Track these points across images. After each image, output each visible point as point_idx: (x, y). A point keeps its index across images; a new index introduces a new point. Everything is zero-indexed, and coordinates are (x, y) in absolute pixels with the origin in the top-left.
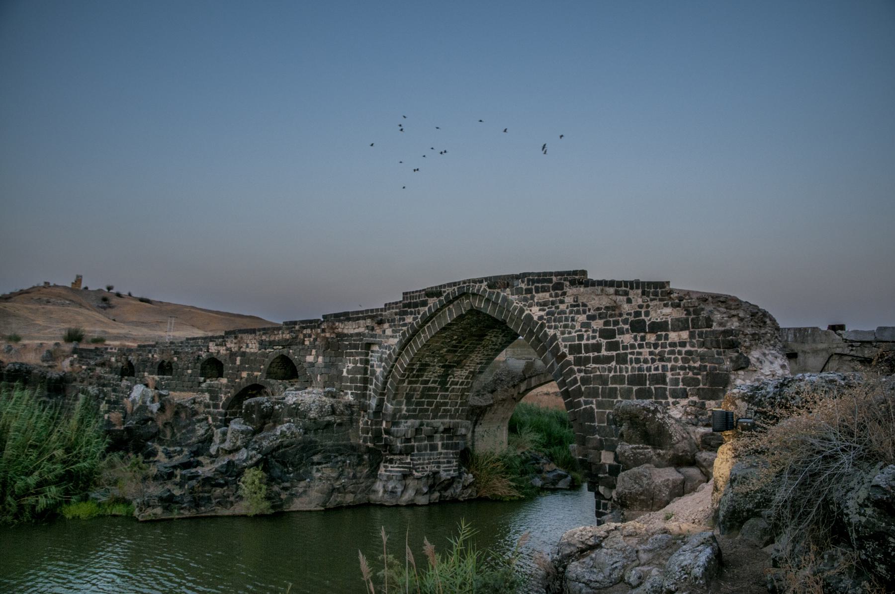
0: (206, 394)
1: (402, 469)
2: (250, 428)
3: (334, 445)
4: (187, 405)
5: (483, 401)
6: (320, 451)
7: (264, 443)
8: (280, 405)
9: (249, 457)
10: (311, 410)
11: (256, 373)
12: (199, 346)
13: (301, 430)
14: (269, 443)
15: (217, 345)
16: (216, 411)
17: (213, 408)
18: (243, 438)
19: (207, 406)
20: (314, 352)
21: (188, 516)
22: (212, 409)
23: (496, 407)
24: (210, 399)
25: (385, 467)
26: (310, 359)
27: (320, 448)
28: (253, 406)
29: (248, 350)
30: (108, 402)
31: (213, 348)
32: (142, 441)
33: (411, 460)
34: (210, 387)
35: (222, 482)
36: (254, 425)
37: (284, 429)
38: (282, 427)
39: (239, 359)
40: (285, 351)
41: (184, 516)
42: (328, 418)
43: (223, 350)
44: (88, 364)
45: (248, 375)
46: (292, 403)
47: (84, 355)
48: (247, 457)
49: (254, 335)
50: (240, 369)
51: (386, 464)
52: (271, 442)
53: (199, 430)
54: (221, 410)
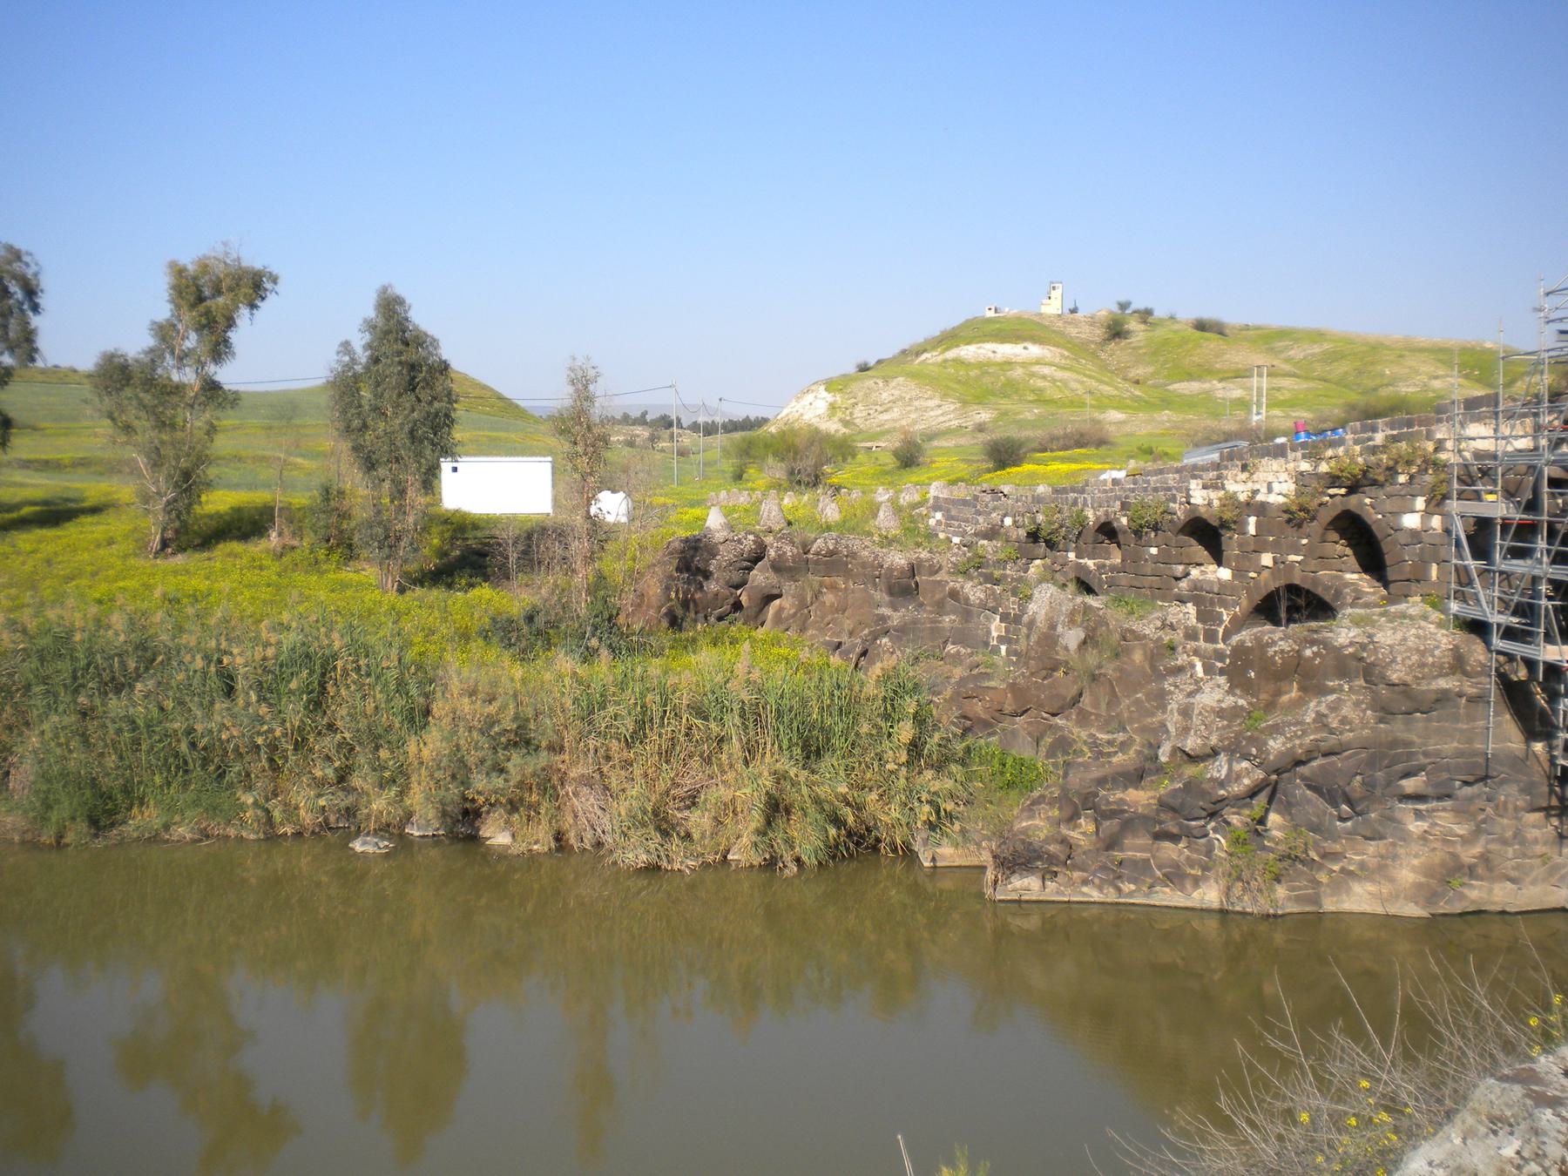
0: (1190, 605)
2: (1241, 702)
3: (1459, 754)
6: (1422, 768)
7: (1271, 743)
8: (1315, 649)
9: (1234, 776)
10: (1393, 661)
12: (1169, 489)
13: (1369, 712)
14: (1284, 744)
15: (1205, 487)
16: (1210, 646)
17: (1205, 641)
18: (1224, 728)
19: (1191, 635)
20: (1420, 503)
21: (1097, 899)
22: (1202, 644)
27: (1423, 760)
31: (1199, 496)
32: (1045, 715)
34: (1196, 588)
35: (1175, 830)
36: (1253, 696)
37: (1323, 709)
39: (1252, 520)
40: (1353, 502)
41: (1092, 900)
42: (1443, 683)
43: (1215, 496)
44: (963, 534)
45: (1275, 561)
48: (1228, 775)
49: (1282, 460)
52: (1290, 739)
53: (1171, 693)
54: (1221, 646)
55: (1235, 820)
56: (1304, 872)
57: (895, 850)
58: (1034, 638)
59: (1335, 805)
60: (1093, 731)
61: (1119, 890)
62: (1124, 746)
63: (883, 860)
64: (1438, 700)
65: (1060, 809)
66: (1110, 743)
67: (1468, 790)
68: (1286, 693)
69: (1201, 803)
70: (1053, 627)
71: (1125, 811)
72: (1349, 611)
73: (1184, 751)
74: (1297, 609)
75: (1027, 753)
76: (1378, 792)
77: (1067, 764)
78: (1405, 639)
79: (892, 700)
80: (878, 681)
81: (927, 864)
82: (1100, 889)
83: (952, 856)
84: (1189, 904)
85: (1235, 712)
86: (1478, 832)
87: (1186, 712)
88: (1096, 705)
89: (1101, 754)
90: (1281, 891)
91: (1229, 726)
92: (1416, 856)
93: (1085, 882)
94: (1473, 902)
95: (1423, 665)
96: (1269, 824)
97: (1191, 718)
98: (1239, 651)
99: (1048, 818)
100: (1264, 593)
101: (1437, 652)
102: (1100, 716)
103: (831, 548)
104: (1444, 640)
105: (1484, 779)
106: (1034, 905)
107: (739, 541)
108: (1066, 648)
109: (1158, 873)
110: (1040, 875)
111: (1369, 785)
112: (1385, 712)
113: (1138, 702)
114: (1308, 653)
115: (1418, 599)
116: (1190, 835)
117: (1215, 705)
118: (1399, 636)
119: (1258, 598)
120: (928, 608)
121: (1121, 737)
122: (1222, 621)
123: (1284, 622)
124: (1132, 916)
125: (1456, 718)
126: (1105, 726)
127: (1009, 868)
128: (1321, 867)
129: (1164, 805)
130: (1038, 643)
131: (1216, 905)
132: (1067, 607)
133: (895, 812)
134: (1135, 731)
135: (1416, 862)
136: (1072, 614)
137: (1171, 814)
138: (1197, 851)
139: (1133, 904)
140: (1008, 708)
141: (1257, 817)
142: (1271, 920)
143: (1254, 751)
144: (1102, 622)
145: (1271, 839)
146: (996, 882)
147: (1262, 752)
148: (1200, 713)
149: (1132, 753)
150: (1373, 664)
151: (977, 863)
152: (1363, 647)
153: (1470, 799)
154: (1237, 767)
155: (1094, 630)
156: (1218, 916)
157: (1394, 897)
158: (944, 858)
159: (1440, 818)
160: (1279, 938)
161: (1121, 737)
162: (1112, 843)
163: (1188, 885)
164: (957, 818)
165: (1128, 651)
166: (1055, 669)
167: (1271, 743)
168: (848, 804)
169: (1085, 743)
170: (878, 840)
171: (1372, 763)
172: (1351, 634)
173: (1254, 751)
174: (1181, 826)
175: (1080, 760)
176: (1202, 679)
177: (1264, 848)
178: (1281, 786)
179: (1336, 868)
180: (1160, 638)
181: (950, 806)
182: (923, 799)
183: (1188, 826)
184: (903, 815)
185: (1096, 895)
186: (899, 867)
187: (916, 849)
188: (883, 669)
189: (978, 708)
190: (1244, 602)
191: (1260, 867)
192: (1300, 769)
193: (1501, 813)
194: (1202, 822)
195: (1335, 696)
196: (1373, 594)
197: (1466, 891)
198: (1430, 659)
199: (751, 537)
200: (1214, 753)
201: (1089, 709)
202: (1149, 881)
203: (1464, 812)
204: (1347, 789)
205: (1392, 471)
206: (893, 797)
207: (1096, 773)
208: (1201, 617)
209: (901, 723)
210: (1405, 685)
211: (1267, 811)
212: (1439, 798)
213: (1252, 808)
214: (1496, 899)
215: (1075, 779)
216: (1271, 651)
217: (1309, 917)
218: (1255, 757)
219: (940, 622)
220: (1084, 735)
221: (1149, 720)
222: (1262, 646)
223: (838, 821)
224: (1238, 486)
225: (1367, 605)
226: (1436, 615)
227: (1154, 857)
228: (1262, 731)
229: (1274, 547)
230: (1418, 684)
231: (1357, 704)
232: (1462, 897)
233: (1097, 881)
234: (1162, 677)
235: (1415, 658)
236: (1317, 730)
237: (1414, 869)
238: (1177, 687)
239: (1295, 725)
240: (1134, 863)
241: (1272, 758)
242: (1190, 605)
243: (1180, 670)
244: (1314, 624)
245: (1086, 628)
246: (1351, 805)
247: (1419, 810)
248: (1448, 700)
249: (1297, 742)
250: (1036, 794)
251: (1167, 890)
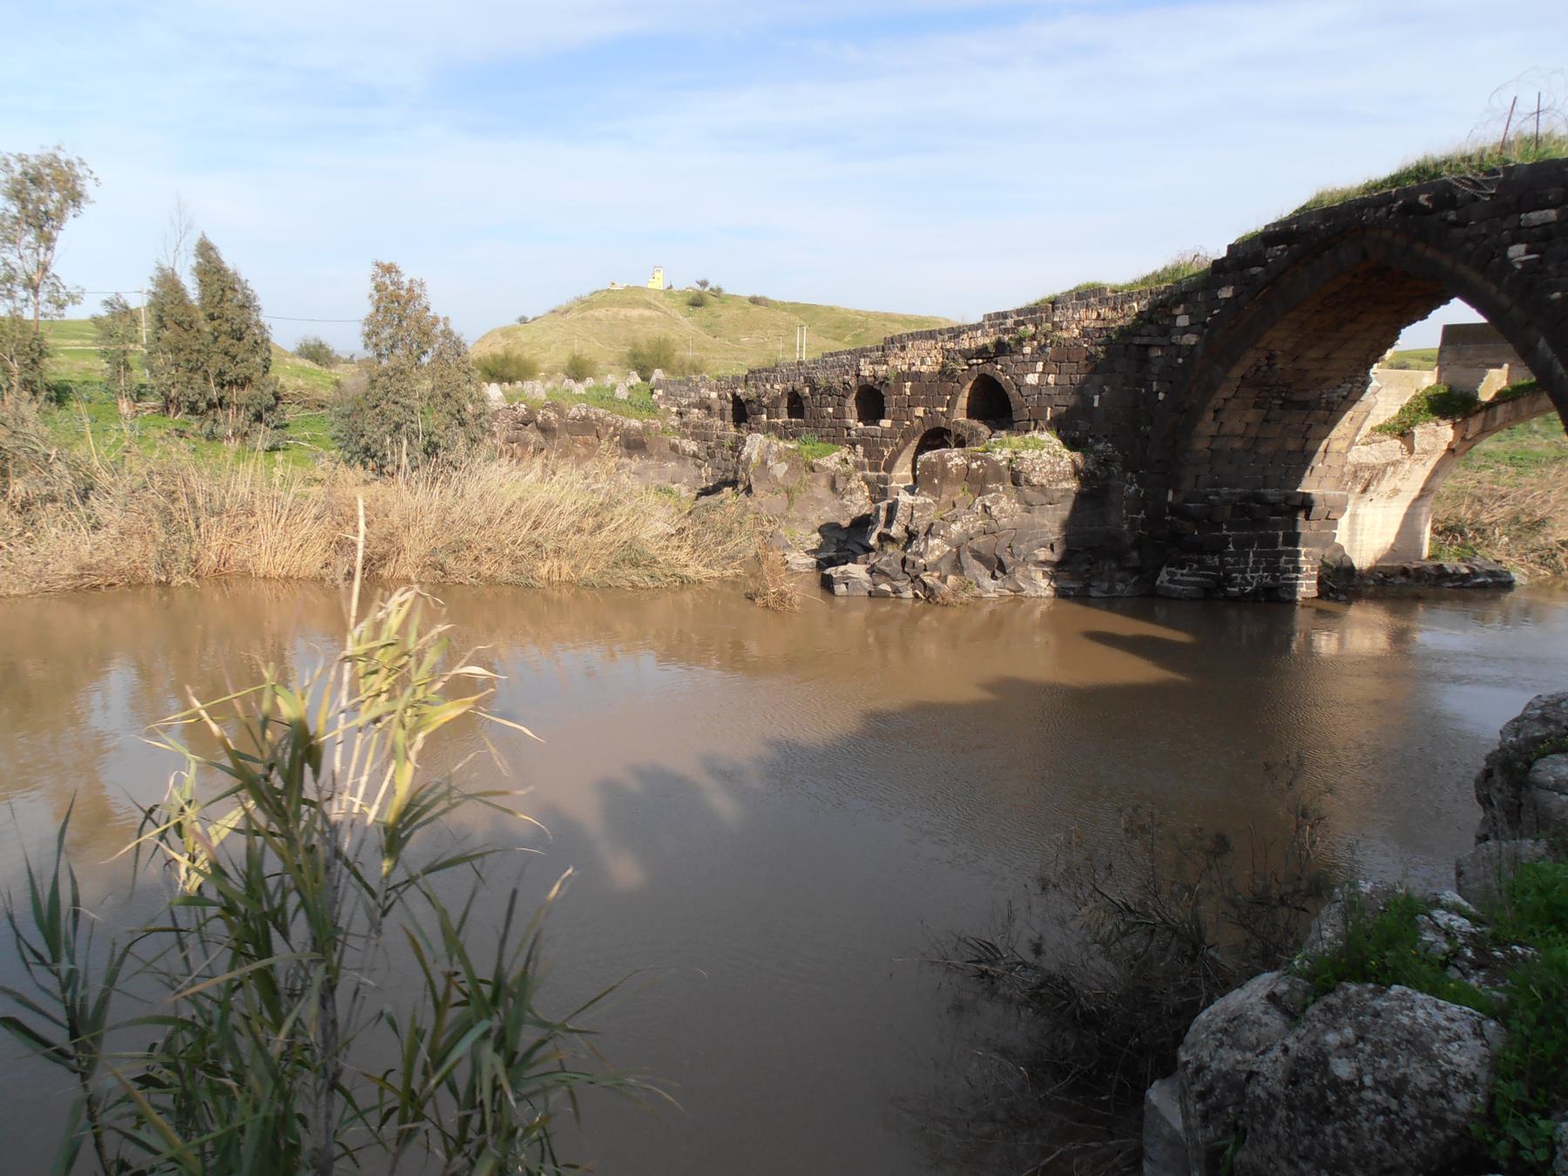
1: (1198, 579)
2: (928, 500)
5: (1377, 454)
8: (979, 463)
10: (1034, 469)
15: (871, 363)
20: (1040, 366)
23: (1407, 467)
25: (1168, 573)
26: (1032, 379)
29: (924, 369)
31: (866, 371)
33: (1221, 562)
47: (671, 389)
50: (912, 404)
51: (1169, 569)
70: (764, 463)
95: (1054, 472)
107: (514, 409)
114: (974, 465)
122: (884, 456)
195: (993, 495)
199: (523, 406)
205: (1020, 341)
208: (867, 454)
210: (1042, 485)
216: (949, 465)
229: (925, 403)
235: (1048, 467)
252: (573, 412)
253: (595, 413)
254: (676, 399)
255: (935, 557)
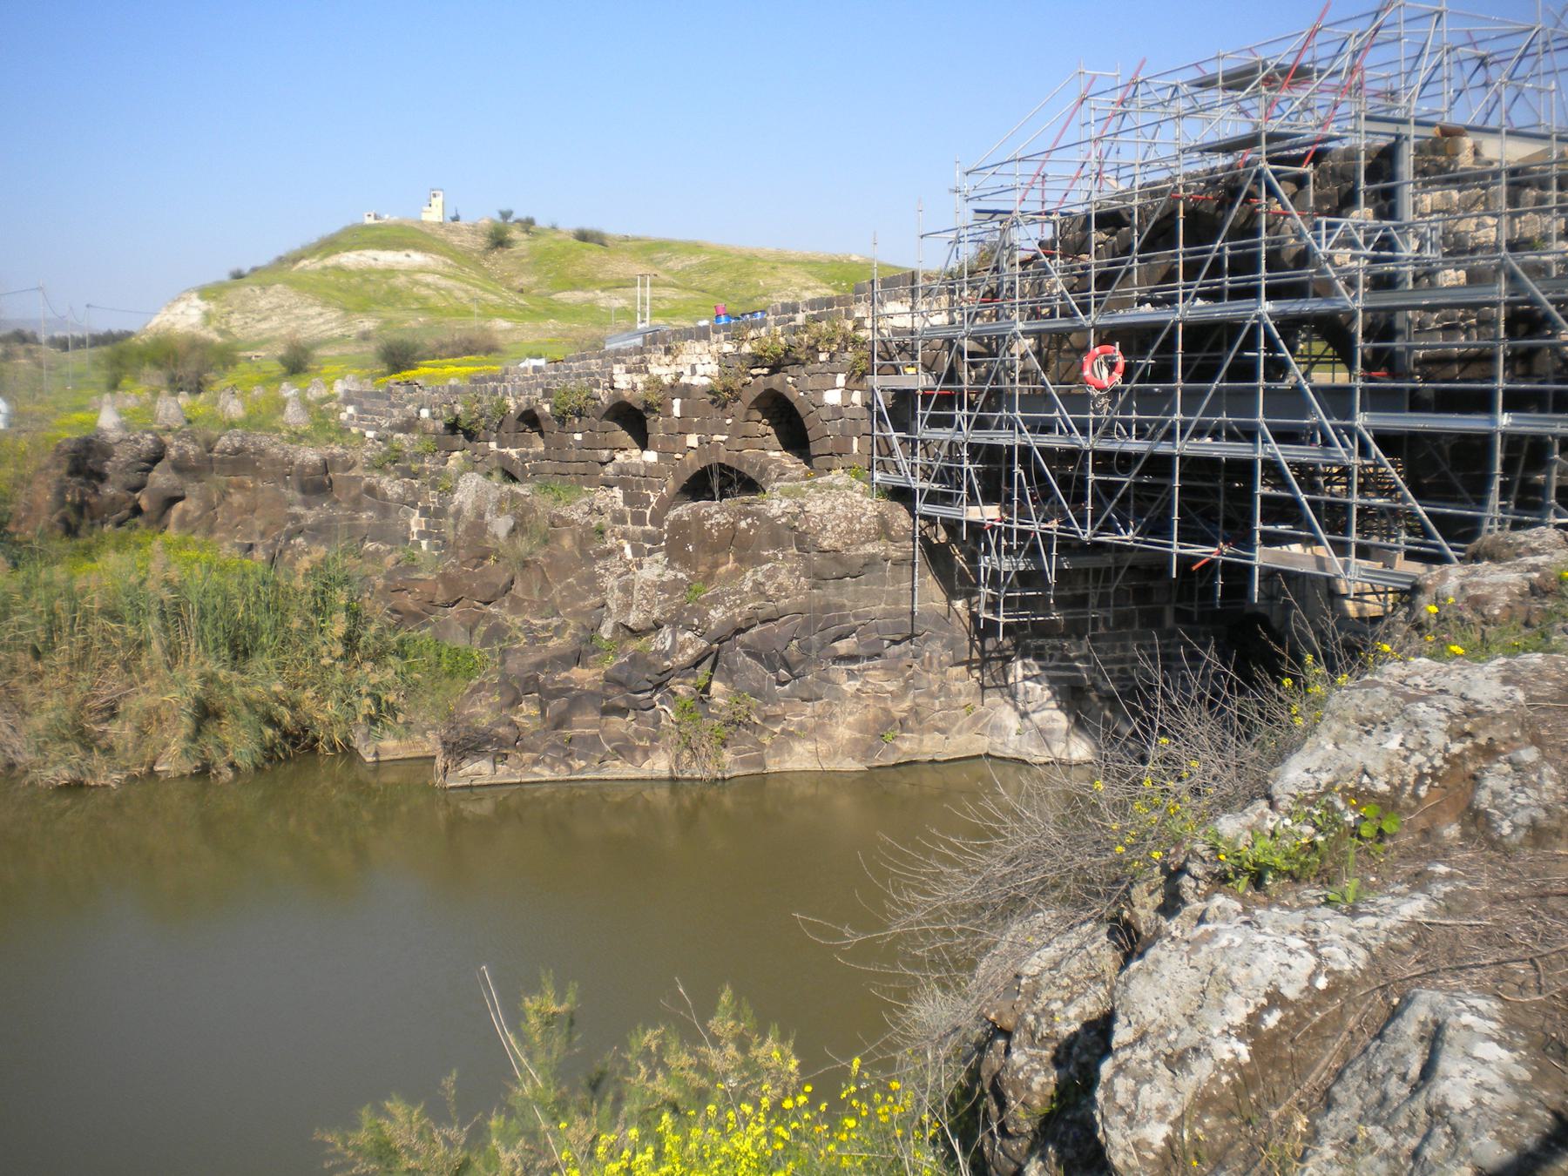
2: (681, 575)
3: (887, 615)
4: (576, 517)
7: (712, 612)
8: (749, 520)
9: (678, 646)
10: (824, 528)
11: (717, 437)
12: (592, 375)
13: (802, 579)
15: (628, 371)
16: (639, 529)
18: (666, 601)
19: (619, 518)
20: (841, 380)
21: (548, 778)
24: (625, 503)
28: (686, 525)
29: (696, 381)
30: (425, 512)
31: (622, 381)
32: (478, 604)
34: (622, 472)
35: (623, 704)
37: (760, 577)
38: (756, 572)
39: (677, 402)
42: (870, 548)
43: (640, 380)
44: (378, 427)
46: (779, 513)
47: (366, 406)
49: (705, 343)
52: (730, 608)
53: (602, 576)
54: (649, 527)
55: (680, 689)
56: (747, 736)
57: (334, 748)
58: (461, 528)
59: (775, 670)
60: (527, 617)
61: (570, 767)
62: (558, 631)
63: (321, 759)
64: (865, 565)
65: (501, 694)
66: (545, 628)
67: (896, 649)
68: (723, 564)
69: (647, 676)
70: (481, 516)
71: (572, 689)
72: (777, 485)
73: (627, 627)
74: (730, 484)
75: (462, 643)
76: (813, 655)
77: (503, 651)
78: (834, 508)
79: (323, 593)
80: (306, 575)
81: (369, 759)
82: (552, 768)
83: (395, 749)
84: (639, 775)
85: (676, 585)
86: (907, 687)
87: (627, 589)
88: (528, 591)
89: (536, 639)
90: (728, 756)
91: (670, 599)
92: (851, 714)
93: (536, 762)
94: (905, 753)
95: (852, 532)
96: (712, 692)
97: (632, 594)
98: (678, 525)
99: (490, 705)
100: (690, 473)
101: (863, 520)
102: (533, 602)
103: (237, 445)
104: (870, 508)
105: (910, 637)
106: (486, 790)
108: (496, 536)
109: (608, 748)
110: (491, 757)
111: (805, 649)
112: (819, 579)
113: (569, 587)
114: (743, 524)
115: (842, 471)
116: (638, 708)
117: (655, 579)
118: (828, 505)
119: (684, 479)
120: (344, 505)
121: (555, 621)
122: (649, 503)
123: (717, 496)
124: (583, 792)
125: (883, 581)
126: (539, 611)
127: (459, 754)
128: (763, 730)
129: (610, 680)
130: (466, 531)
131: (666, 774)
132: (494, 495)
133: (331, 707)
134: (567, 615)
135: (851, 719)
136: (500, 501)
137: (617, 689)
138: (645, 723)
139: (584, 780)
140: (439, 599)
141: (703, 684)
142: (719, 784)
143: (696, 621)
144: (530, 509)
145: (716, 706)
146: (446, 769)
147: (704, 622)
148: (642, 588)
149: (567, 637)
150: (805, 533)
151: (421, 754)
152: (795, 517)
153: (899, 657)
154: (680, 638)
155: (522, 517)
156: (667, 785)
157: (832, 754)
158: (387, 751)
159: (871, 676)
160: (728, 801)
161: (555, 621)
162: (561, 722)
163: (639, 756)
164: (399, 710)
165: (556, 537)
166: (485, 557)
167: (712, 612)
168: (282, 703)
169: (520, 629)
170: (316, 740)
171: (807, 627)
172: (783, 505)
173: (696, 621)
174: (627, 698)
175: (516, 646)
176: (631, 561)
177: (709, 715)
178: (722, 654)
179: (777, 730)
180: (589, 523)
181: (392, 698)
182: (363, 692)
183: (635, 700)
184: (341, 711)
185: (546, 774)
186: (339, 765)
187: (355, 746)
188: (311, 562)
189: (409, 601)
190: (671, 483)
191: (707, 733)
192: (740, 637)
193: (927, 668)
194: (648, 694)
195: (770, 565)
196: (797, 469)
197: (898, 743)
198: (858, 526)
199: (149, 436)
200: (658, 626)
201: (521, 596)
202: (599, 756)
203: (893, 669)
204: (785, 653)
205: (814, 350)
206: (328, 694)
207: (534, 658)
208: (628, 500)
209: (334, 616)
211: (710, 678)
212: (870, 658)
213: (696, 677)
214: (926, 749)
215: (513, 665)
216: (707, 525)
217: (755, 778)
218: (698, 628)
219: (356, 519)
220: (518, 621)
221: (581, 604)
222: (699, 520)
223: (271, 721)
224: (662, 369)
225: (791, 480)
226: (859, 486)
227: (602, 732)
228: (702, 602)
229: (700, 428)
230: (848, 550)
231: (791, 571)
232: (896, 749)
233: (548, 760)
234: (593, 561)
235: (843, 525)
236: (755, 599)
237: (849, 726)
238: (607, 570)
239: (734, 594)
240: (583, 739)
241: (713, 627)
242: (616, 489)
243: (610, 553)
244: (746, 498)
245: (515, 515)
246: (789, 670)
247: (852, 671)
248: (875, 564)
249: (737, 610)
250: (474, 682)
251: (617, 763)
252: (225, 441)
253: (254, 444)
254: (373, 420)
255: (686, 657)
